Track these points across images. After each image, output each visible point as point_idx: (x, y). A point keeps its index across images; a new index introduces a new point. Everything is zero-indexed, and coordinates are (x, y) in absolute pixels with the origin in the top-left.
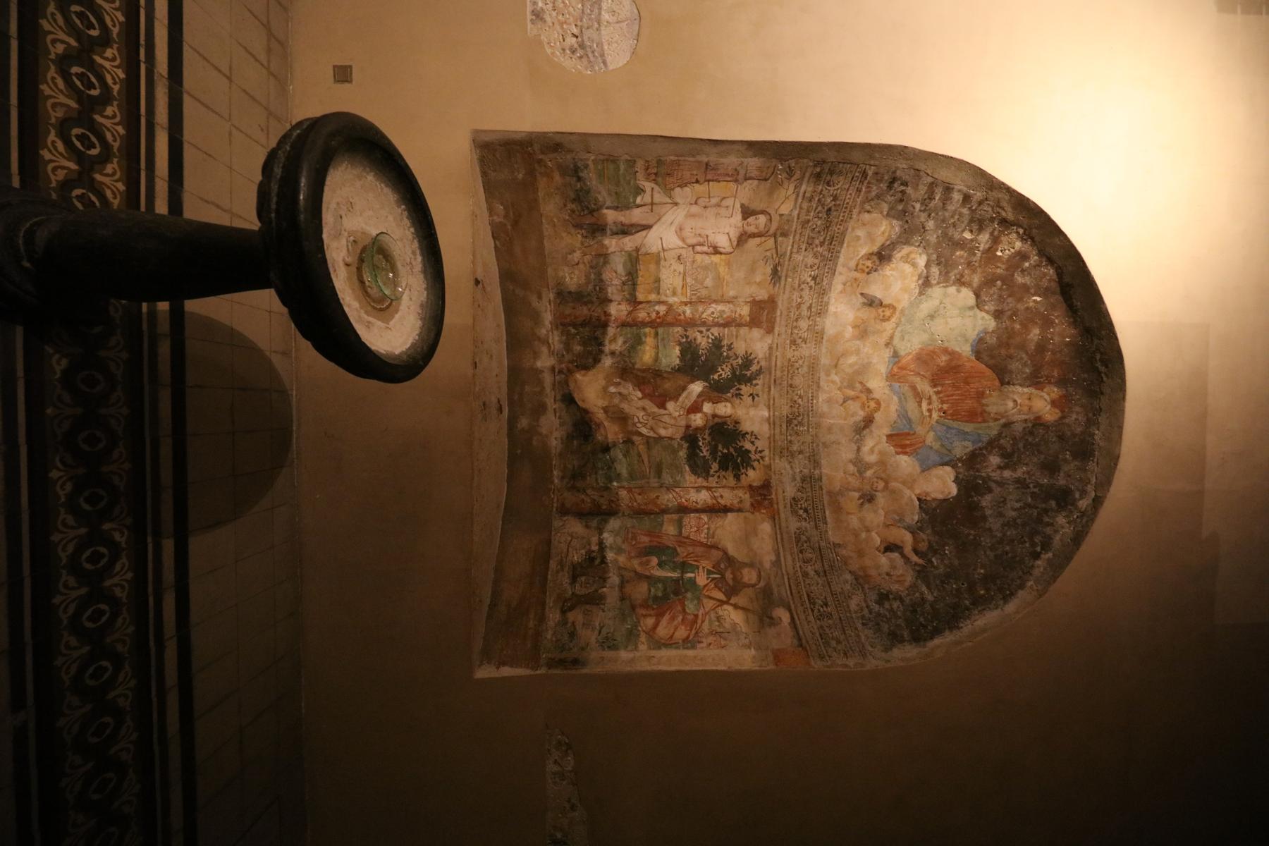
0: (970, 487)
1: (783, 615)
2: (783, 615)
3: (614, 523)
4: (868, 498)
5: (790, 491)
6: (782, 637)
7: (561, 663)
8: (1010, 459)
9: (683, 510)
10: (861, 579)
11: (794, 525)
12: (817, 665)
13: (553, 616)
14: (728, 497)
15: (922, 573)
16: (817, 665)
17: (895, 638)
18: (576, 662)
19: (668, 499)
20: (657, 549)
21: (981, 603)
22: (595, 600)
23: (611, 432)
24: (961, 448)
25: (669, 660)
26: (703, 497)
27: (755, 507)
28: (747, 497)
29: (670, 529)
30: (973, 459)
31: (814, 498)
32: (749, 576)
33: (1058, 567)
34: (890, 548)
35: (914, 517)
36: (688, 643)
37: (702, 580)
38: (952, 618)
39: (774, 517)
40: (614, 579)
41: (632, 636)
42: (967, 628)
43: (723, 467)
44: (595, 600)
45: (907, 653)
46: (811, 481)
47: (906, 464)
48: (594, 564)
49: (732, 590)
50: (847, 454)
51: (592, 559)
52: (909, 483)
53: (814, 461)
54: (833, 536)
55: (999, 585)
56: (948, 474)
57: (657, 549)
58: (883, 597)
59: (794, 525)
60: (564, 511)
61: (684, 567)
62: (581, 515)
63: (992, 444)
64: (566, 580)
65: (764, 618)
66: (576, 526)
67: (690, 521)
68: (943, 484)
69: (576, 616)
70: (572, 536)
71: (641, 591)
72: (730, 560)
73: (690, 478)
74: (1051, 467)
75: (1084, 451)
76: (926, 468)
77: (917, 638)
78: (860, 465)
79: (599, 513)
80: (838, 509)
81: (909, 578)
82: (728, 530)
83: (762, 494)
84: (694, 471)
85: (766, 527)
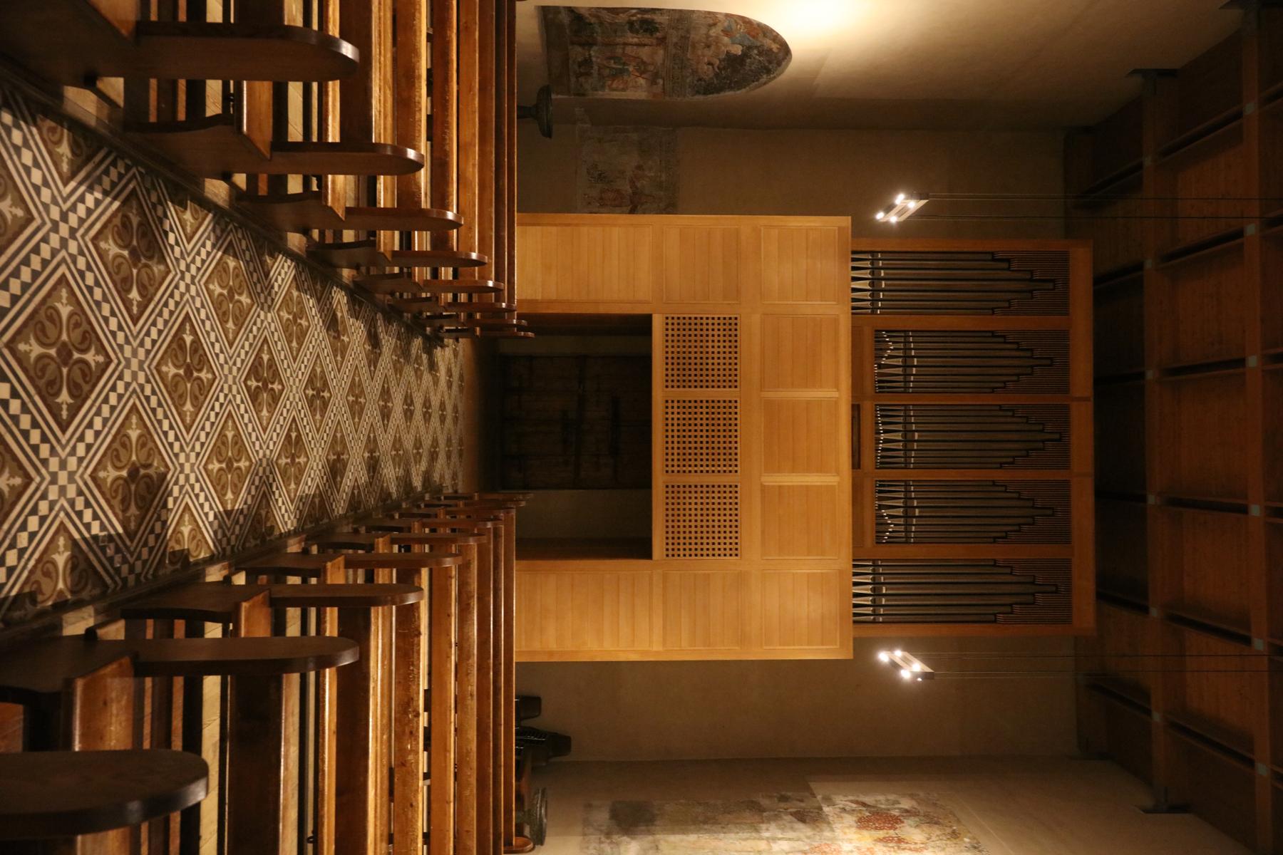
0: (745, 55)
1: (661, 81)
2: (661, 81)
3: (595, 48)
4: (709, 47)
5: (675, 40)
6: (658, 89)
7: (578, 95)
8: (760, 54)
9: (626, 44)
10: (694, 72)
11: (674, 51)
12: (667, 98)
13: (573, 79)
14: (646, 41)
15: (717, 75)
16: (667, 98)
17: (698, 93)
18: (584, 95)
19: (618, 40)
20: (616, 59)
21: (731, 88)
22: (588, 74)
23: (593, 20)
24: (747, 43)
25: (616, 95)
26: (636, 40)
27: (658, 45)
28: (655, 42)
29: (619, 51)
30: (750, 48)
31: (685, 42)
32: (651, 68)
33: (756, 87)
34: (709, 64)
35: (723, 56)
36: (623, 90)
37: (631, 69)
38: (719, 90)
39: (666, 49)
40: (596, 67)
41: (603, 87)
42: (722, 94)
43: (646, 31)
44: (588, 74)
45: (700, 98)
46: (685, 38)
47: (726, 39)
48: (587, 62)
49: (642, 73)
50: (703, 31)
51: (586, 60)
52: (726, 46)
53: (688, 31)
54: (689, 56)
55: (739, 85)
56: (740, 48)
57: (616, 59)
58: (700, 80)
59: (674, 51)
60: (573, 43)
61: (624, 64)
62: (582, 45)
63: (757, 47)
64: (576, 67)
65: (653, 82)
66: (579, 49)
67: (629, 49)
68: (737, 50)
69: (582, 79)
70: (577, 53)
71: (607, 72)
72: (644, 63)
73: (629, 34)
74: (770, 62)
75: (779, 64)
76: (733, 43)
77: (705, 94)
78: (708, 36)
79: (589, 44)
80: (694, 46)
81: (712, 75)
82: (644, 53)
83: (662, 41)
84: (632, 31)
85: (661, 52)
